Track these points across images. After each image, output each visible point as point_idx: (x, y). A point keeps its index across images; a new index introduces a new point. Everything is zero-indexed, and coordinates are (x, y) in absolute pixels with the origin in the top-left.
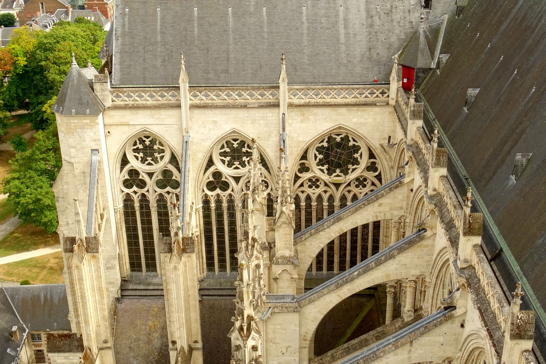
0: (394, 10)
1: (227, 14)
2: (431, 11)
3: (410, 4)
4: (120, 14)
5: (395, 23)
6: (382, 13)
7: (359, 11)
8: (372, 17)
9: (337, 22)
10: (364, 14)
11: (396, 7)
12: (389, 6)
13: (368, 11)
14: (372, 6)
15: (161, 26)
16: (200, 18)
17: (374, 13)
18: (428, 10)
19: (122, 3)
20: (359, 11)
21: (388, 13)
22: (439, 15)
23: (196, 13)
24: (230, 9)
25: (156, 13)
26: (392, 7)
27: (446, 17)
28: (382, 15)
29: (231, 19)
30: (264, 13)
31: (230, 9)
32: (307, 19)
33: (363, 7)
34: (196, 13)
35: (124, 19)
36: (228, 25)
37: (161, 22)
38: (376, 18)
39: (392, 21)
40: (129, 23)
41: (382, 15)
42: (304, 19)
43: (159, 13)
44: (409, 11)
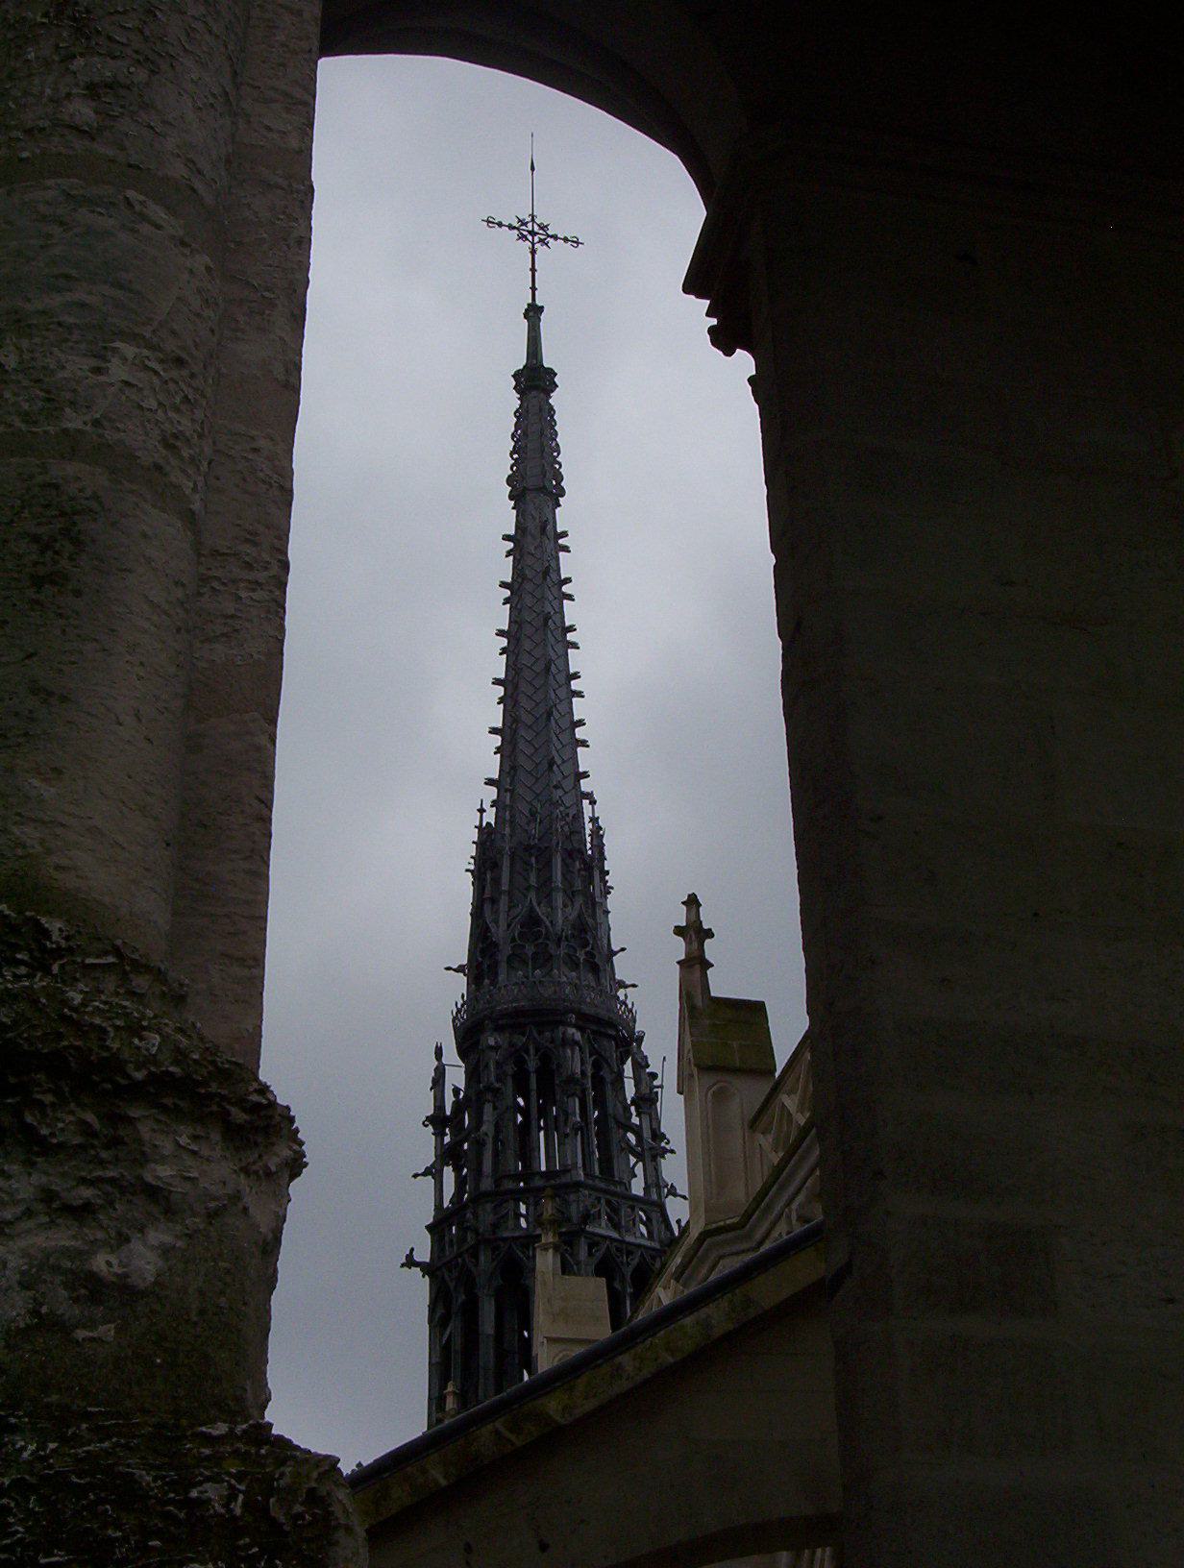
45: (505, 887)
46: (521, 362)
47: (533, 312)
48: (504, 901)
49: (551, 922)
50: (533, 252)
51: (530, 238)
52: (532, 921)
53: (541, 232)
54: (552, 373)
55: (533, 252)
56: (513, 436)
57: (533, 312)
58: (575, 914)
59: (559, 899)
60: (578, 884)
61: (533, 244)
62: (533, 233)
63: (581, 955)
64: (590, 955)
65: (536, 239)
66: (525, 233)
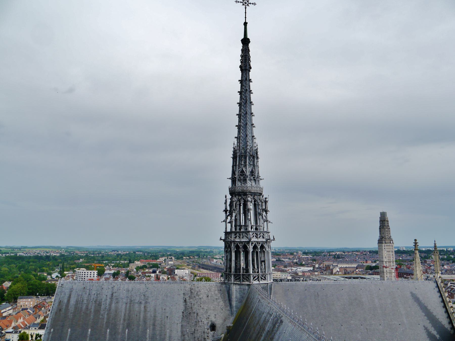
0: (196, 332)
1: (106, 333)
2: (216, 332)
3: (205, 329)
4: (48, 332)
5: (196, 339)
6: (190, 333)
7: (177, 332)
8: (184, 335)
9: (165, 338)
10: (180, 334)
11: (197, 330)
12: (193, 330)
13: (182, 332)
14: (185, 330)
15: (69, 339)
16: (91, 335)
17: (185, 333)
18: (214, 332)
19: (50, 326)
20: (177, 332)
21: (193, 334)
22: (219, 335)
23: (89, 332)
24: (108, 330)
25: (68, 332)
26: (195, 330)
27: (223, 335)
28: (190, 335)
29: (108, 336)
30: (127, 333)
31: (108, 330)
32: (149, 336)
33: (179, 330)
34: (89, 332)
35: (49, 335)
36: (105, 340)
37: (69, 337)
38: (186, 336)
39: (195, 337)
40: (52, 337)
41: (190, 335)
42: (148, 336)
43: (69, 332)
44: (204, 332)
45: (238, 164)
46: (243, 37)
47: (245, 24)
48: (237, 167)
49: (246, 172)
50: (246, 8)
51: (245, 4)
52: (242, 171)
53: (247, 2)
54: (249, 39)
55: (246, 8)
56: (241, 56)
57: (245, 24)
58: (251, 169)
59: (248, 167)
60: (252, 163)
61: (246, 6)
62: (246, 3)
63: (252, 178)
64: (254, 178)
65: (246, 5)
66: (244, 3)
